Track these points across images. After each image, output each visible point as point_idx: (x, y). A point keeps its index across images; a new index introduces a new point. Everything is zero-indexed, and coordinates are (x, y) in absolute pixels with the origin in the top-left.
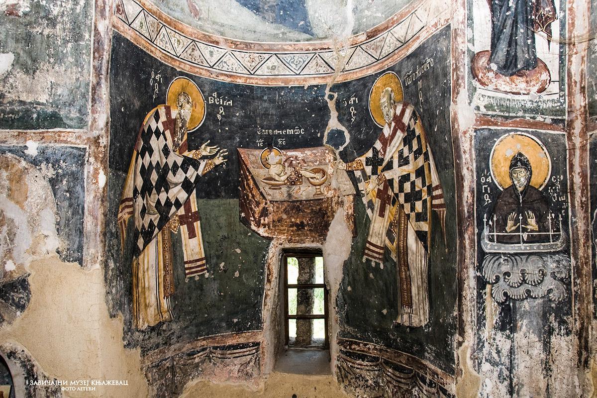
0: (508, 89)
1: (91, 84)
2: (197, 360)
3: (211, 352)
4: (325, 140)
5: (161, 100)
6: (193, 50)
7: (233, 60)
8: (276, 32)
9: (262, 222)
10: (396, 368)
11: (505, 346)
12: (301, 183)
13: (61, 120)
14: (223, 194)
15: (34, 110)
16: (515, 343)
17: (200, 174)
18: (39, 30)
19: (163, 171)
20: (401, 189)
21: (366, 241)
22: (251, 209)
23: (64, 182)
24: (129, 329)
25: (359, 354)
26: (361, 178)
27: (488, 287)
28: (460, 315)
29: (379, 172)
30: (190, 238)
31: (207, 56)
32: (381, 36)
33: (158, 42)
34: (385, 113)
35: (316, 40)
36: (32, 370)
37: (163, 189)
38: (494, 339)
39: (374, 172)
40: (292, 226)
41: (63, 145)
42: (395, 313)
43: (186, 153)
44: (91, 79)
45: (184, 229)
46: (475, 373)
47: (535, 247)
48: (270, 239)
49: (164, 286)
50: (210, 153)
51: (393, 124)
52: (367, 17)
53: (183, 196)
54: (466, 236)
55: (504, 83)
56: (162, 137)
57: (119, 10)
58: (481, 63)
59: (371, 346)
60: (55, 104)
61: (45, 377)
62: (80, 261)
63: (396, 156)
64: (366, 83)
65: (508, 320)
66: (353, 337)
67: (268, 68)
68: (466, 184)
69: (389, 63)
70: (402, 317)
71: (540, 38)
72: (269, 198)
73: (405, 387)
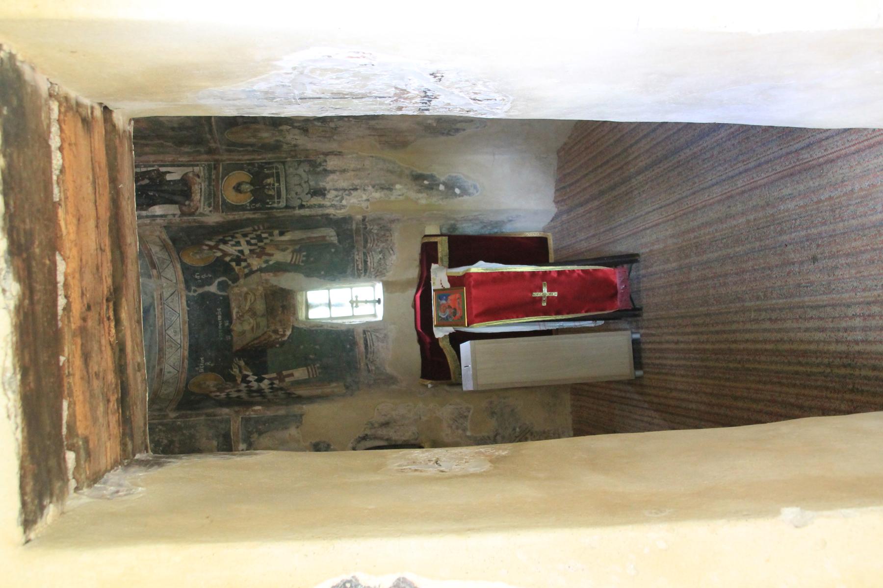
7: (172, 359)
10: (366, 242)
11: (333, 193)
19: (250, 391)
20: (256, 244)
24: (344, 396)
31: (171, 375)
39: (245, 260)
42: (333, 245)
45: (287, 380)
47: (282, 179)
48: (293, 328)
53: (266, 382)
55: (196, 197)
59: (357, 257)
62: (301, 415)
64: (187, 270)
65: (320, 192)
68: (251, 216)
69: (175, 255)
71: (169, 177)
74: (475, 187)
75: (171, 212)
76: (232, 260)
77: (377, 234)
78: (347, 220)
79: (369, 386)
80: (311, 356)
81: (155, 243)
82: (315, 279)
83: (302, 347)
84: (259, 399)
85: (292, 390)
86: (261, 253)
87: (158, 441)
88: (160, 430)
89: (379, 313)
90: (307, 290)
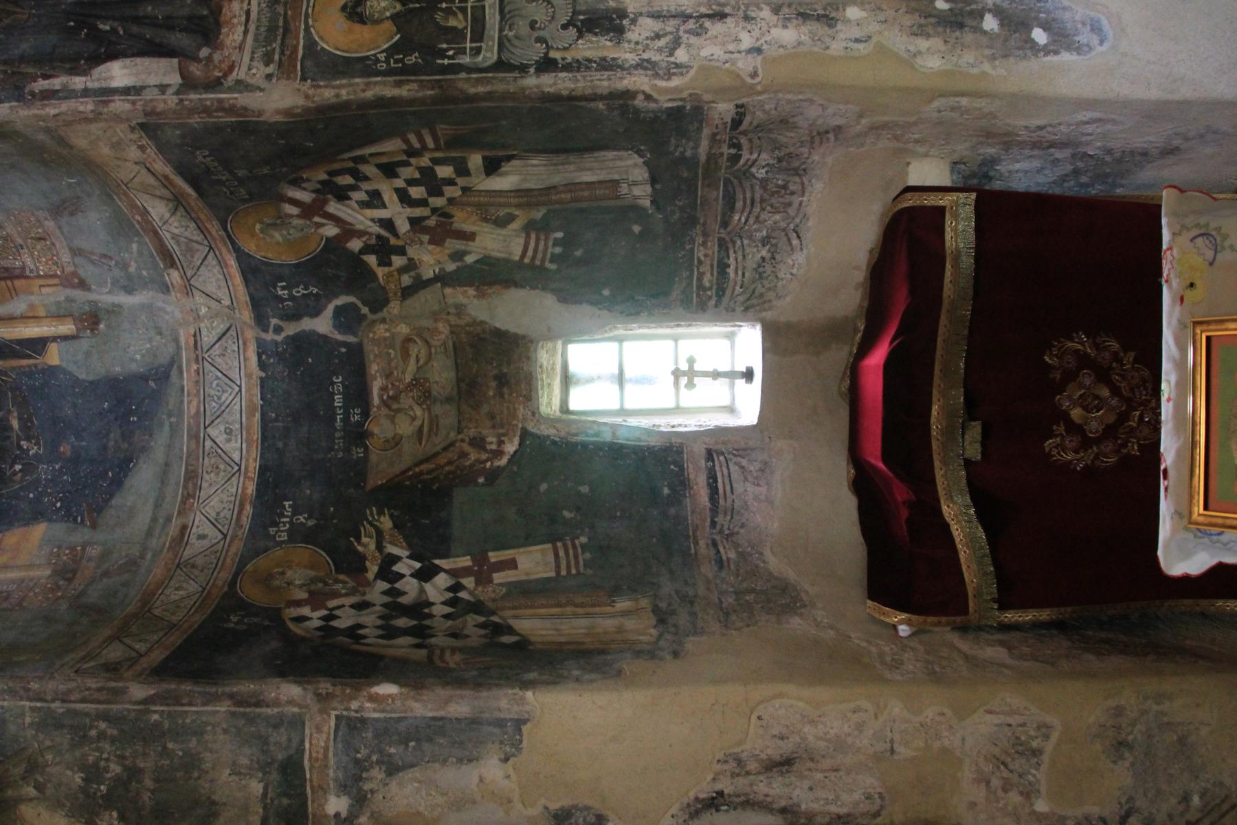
0: (241, 29)
1: (233, 709)
2: (732, 555)
3: (721, 532)
4: (351, 339)
5: (275, 615)
6: (194, 566)
7: (214, 502)
8: (166, 428)
9: (494, 447)
11: (647, 26)
12: (427, 380)
13: (290, 757)
14: (443, 514)
15: (276, 802)
16: (644, 10)
17: (407, 553)
18: (146, 796)
19: (394, 608)
20: (423, 203)
21: (520, 264)
22: (471, 466)
23: (392, 750)
24: (650, 653)
25: (719, 273)
26: (412, 274)
27: (553, 54)
28: (602, 98)
29: (400, 243)
30: (516, 567)
32: (170, 243)
33: (175, 619)
34: (300, 234)
35: (181, 359)
36: (703, 800)
37: (426, 610)
38: (637, 43)
39: (401, 251)
40: (502, 395)
41: (331, 754)
42: (635, 210)
43: (370, 575)
44: (223, 709)
45: (498, 577)
46: (692, 72)
48: (525, 434)
49: (593, 606)
50: (371, 537)
51: (317, 219)
52: (139, 268)
53: (442, 580)
54: (472, 91)
55: (233, 36)
56: (337, 612)
57: (115, 669)
58: (198, 73)
59: (700, 253)
60: (264, 767)
61: (714, 779)
62: (519, 723)
63: (369, 213)
64: (251, 270)
66: (690, 284)
67: (229, 441)
68: (390, 92)
69: (214, 228)
70: (639, 198)
72: (452, 434)
73: (759, 193)
74: (1096, 28)
75: (153, 80)
76: (367, 249)
77: (764, 182)
78: (684, 118)
79: (725, 616)
80: (566, 514)
81: (146, 189)
82: (586, 309)
83: (544, 487)
84: (403, 646)
85: (507, 616)
86: (440, 230)
87: (96, 765)
88: (102, 736)
89: (747, 406)
90: (570, 336)
